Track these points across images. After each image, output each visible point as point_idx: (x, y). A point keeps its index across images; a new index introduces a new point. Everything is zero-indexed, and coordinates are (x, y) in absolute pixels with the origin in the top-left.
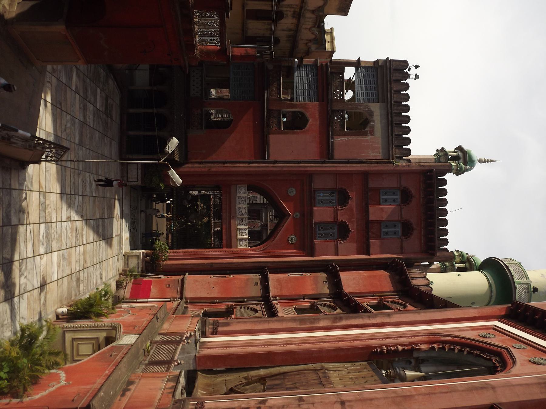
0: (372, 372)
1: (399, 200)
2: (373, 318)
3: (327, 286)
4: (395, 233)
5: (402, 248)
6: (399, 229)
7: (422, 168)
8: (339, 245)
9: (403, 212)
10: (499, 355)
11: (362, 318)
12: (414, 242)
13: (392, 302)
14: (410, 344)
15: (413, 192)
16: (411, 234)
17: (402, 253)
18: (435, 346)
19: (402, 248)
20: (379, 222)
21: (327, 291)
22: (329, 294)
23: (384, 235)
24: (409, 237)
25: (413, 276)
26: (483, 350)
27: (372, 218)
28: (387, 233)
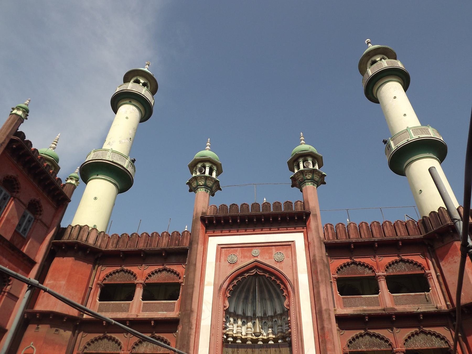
0: (240, 350)
1: (8, 193)
2: (191, 325)
3: (61, 331)
4: (29, 221)
5: (45, 225)
6: (29, 215)
7: (5, 146)
8: (12, 292)
9: (22, 200)
10: (256, 267)
11: (190, 334)
12: (47, 209)
13: (107, 276)
14: (224, 310)
15: (12, 173)
16: (40, 207)
17: (48, 229)
18: (229, 295)
19: (45, 225)
20: (16, 232)
21: (68, 334)
22: (74, 333)
23: (25, 234)
24: (41, 211)
25: (84, 239)
26: (247, 271)
27: (8, 237)
28: (25, 230)
